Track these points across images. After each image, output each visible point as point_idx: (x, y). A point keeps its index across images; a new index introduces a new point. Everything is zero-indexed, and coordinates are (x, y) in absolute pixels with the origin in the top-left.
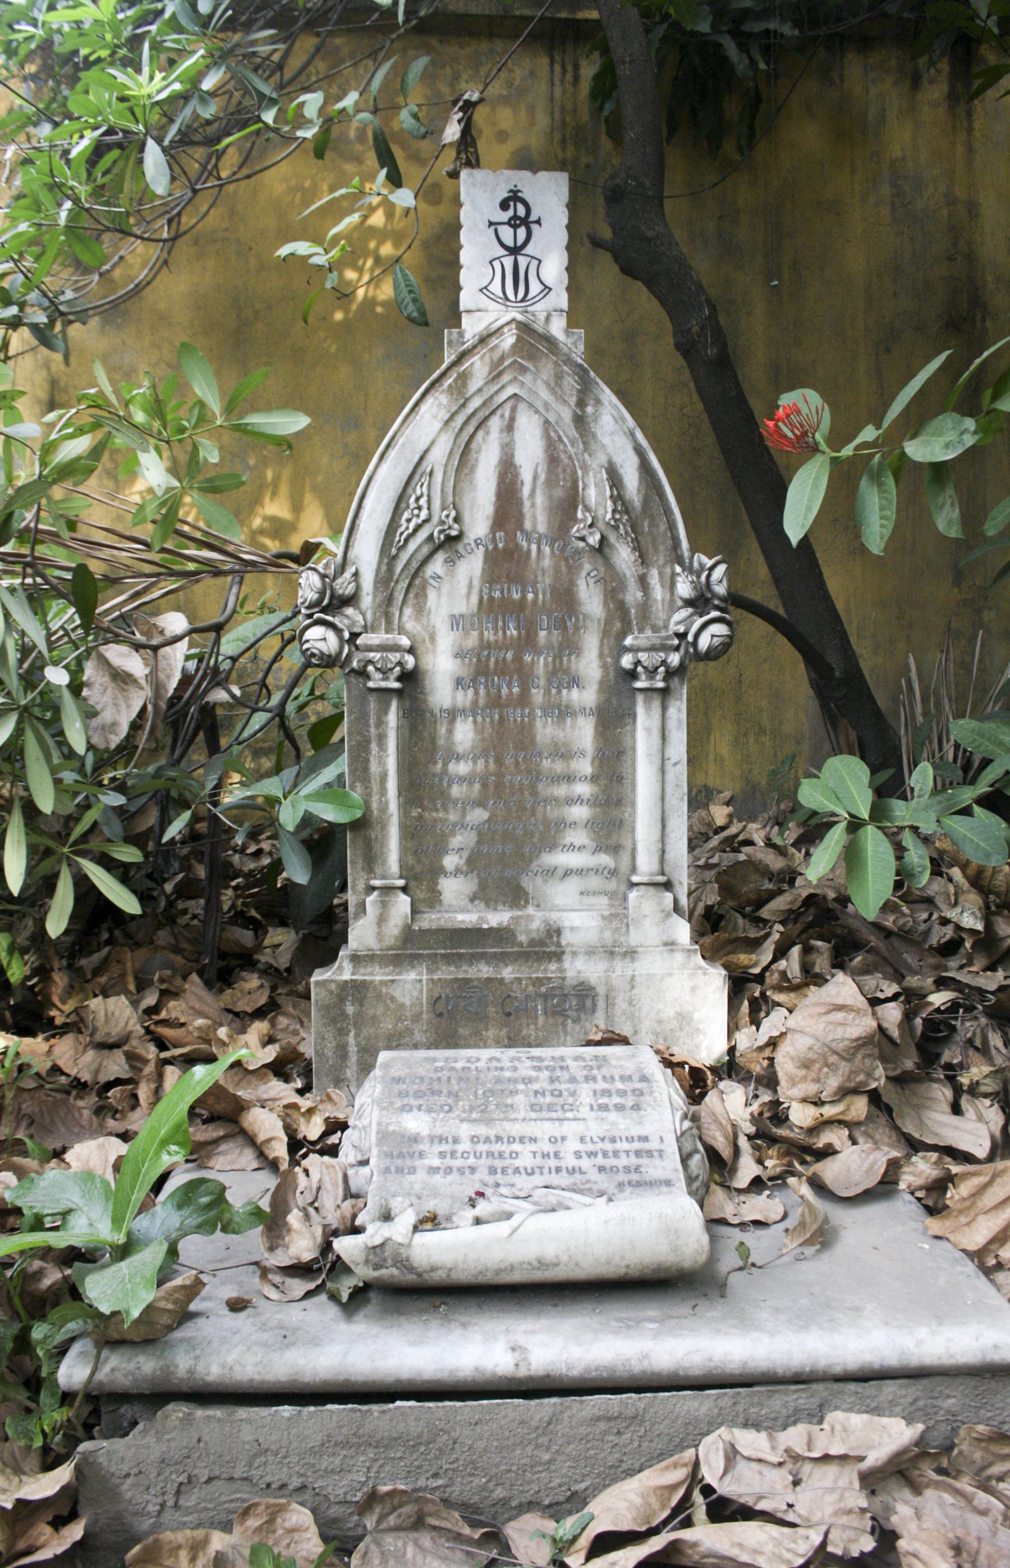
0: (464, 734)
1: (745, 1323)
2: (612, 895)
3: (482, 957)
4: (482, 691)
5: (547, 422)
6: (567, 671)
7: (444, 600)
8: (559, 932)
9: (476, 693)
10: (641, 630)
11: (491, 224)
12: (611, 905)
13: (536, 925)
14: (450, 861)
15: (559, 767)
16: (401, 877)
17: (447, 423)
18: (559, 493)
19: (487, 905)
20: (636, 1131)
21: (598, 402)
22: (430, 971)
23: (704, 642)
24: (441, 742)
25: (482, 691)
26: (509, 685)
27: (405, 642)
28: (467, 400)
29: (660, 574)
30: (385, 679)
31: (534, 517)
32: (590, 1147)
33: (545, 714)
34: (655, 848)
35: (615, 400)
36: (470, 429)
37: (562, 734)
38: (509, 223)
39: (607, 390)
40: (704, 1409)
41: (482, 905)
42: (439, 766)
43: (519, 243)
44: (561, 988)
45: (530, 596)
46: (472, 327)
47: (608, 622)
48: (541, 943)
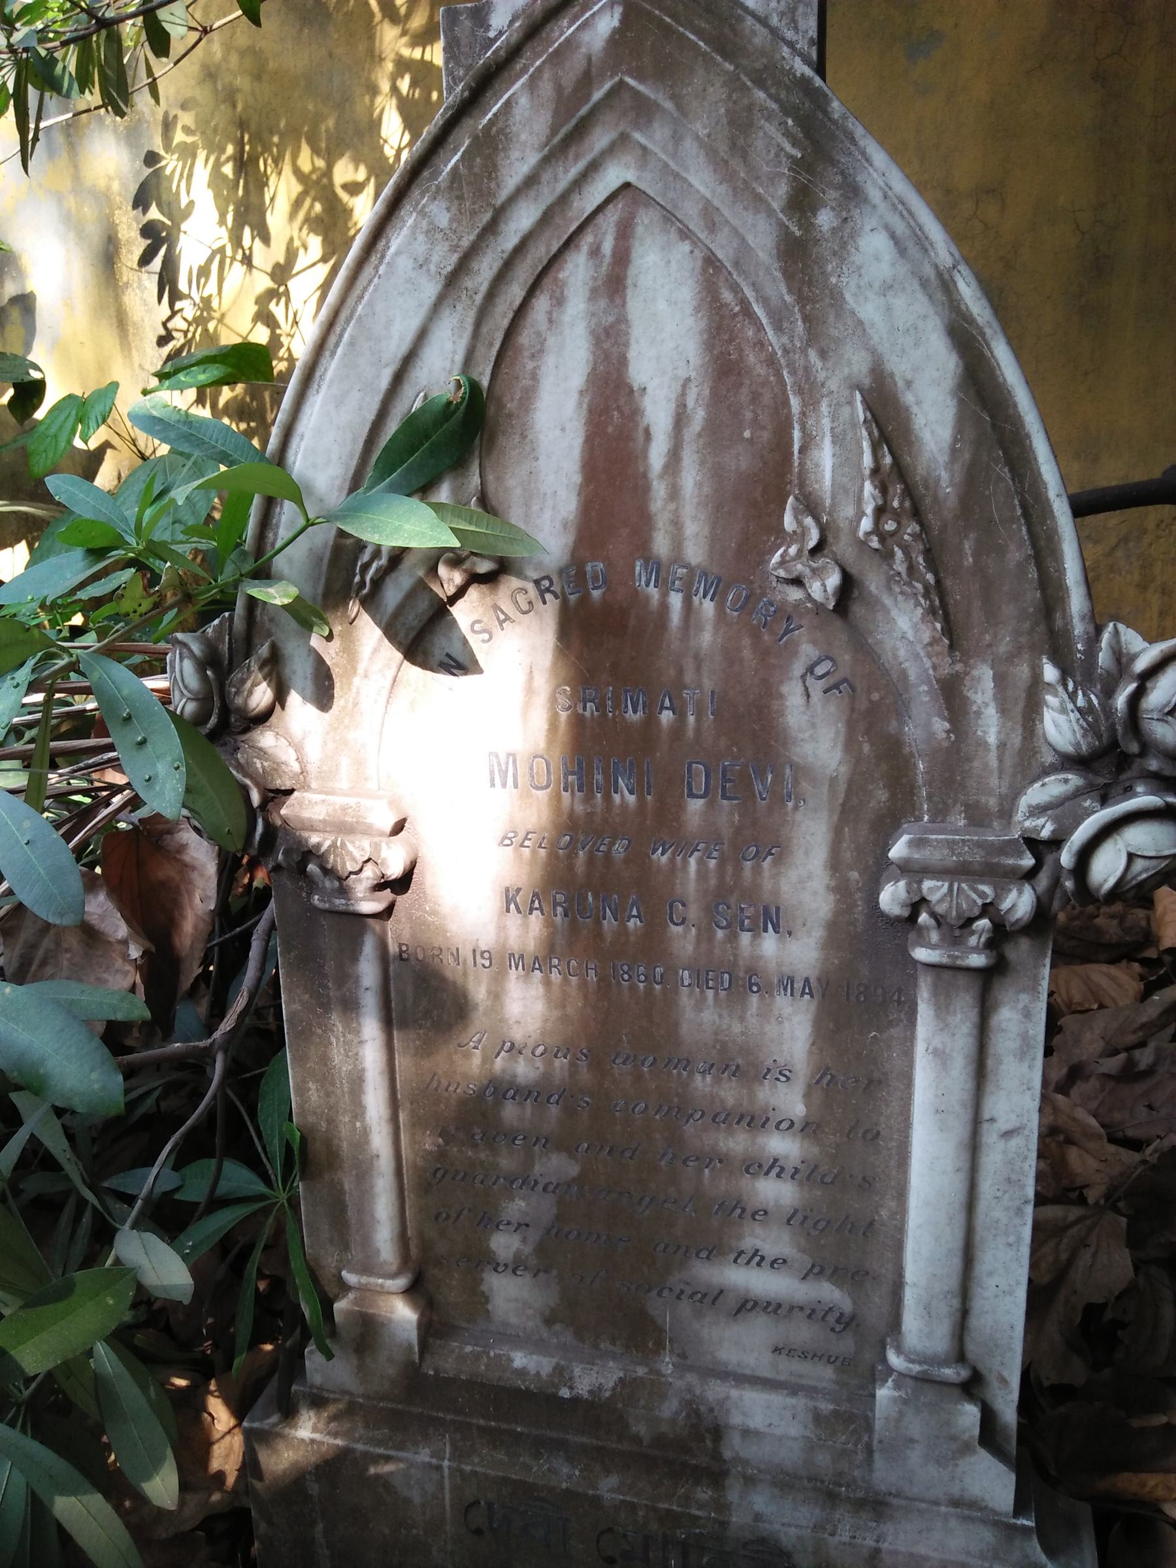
2: (844, 1365)
5: (711, 262)
6: (751, 894)
10: (940, 813)
13: (669, 1408)
15: (730, 1094)
17: (453, 280)
18: (740, 460)
19: (579, 1335)
21: (853, 193)
22: (459, 1454)
23: (1107, 867)
26: (620, 915)
28: (499, 215)
31: (677, 524)
33: (701, 979)
34: (946, 1309)
35: (901, 186)
36: (515, 292)
37: (737, 1028)
39: (879, 157)
41: (568, 1337)
45: (666, 717)
47: (856, 788)
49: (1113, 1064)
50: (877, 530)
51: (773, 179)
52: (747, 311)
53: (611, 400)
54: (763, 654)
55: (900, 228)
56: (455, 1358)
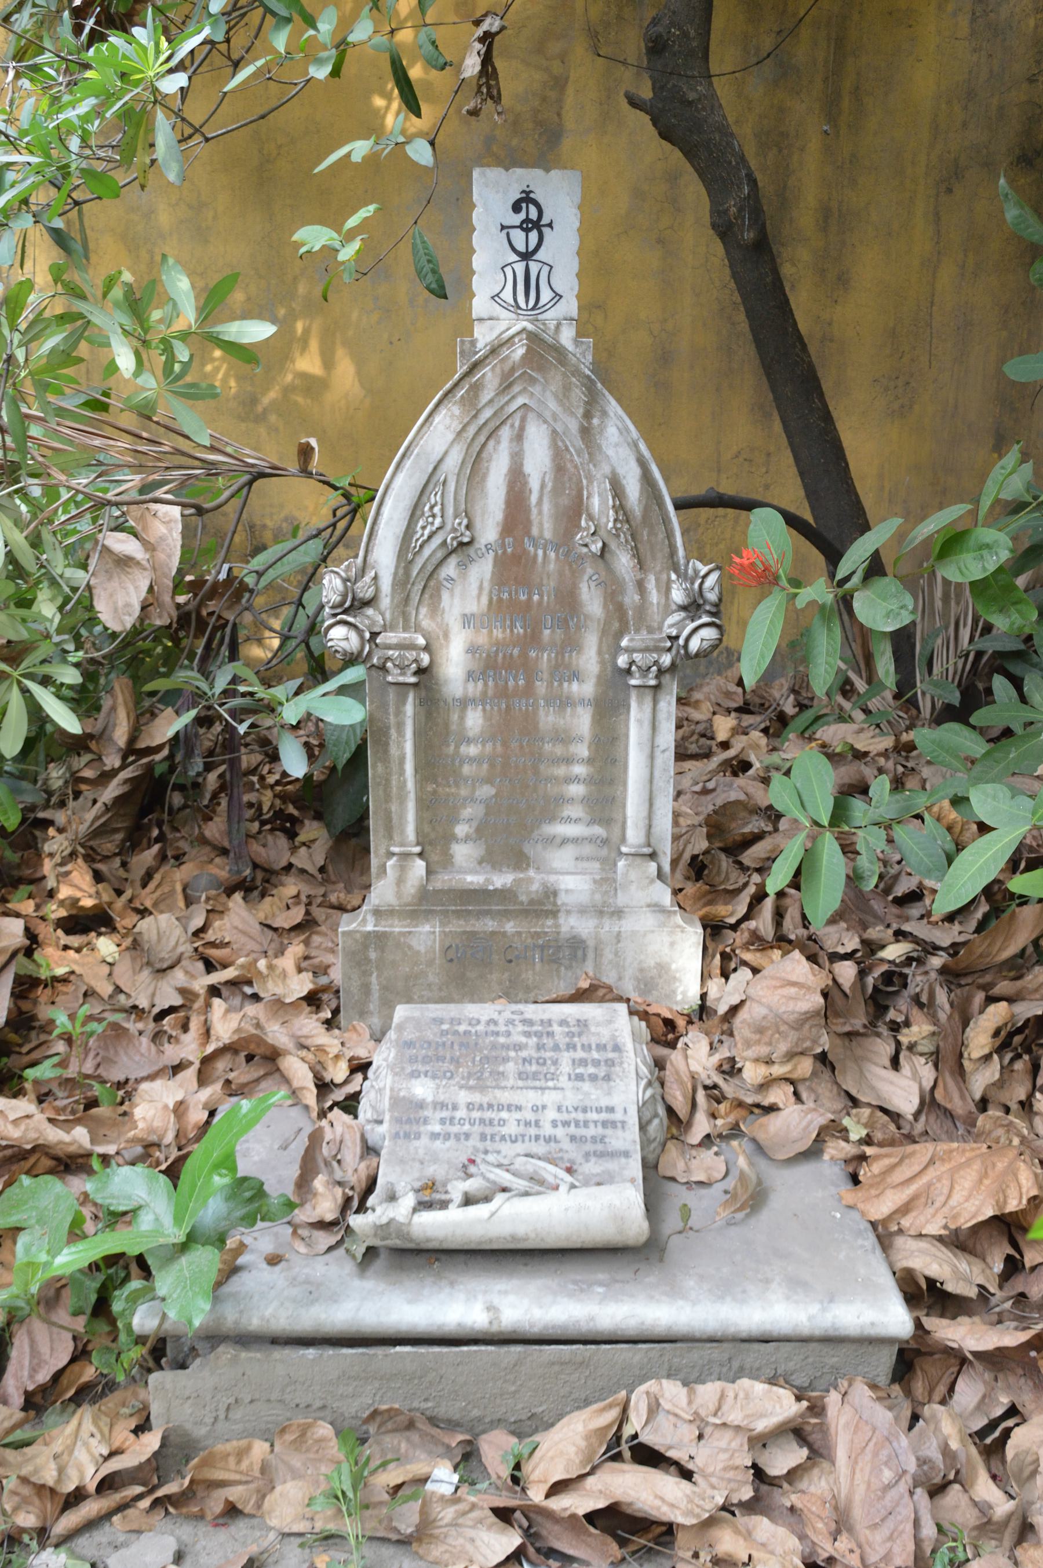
0: (474, 720)
1: (675, 1292)
2: (604, 861)
3: (488, 913)
4: (491, 683)
6: (568, 667)
7: (457, 601)
8: (555, 893)
9: (486, 684)
10: (637, 631)
11: (503, 227)
12: (603, 869)
13: (535, 887)
14: (461, 830)
15: (559, 750)
16: (418, 844)
17: (459, 434)
18: (565, 501)
19: (493, 867)
20: (604, 1102)
21: (604, 413)
23: (694, 645)
24: (454, 727)
25: (491, 683)
27: (421, 641)
28: (478, 412)
29: (657, 580)
30: (403, 674)
31: (541, 524)
32: (565, 1117)
33: (548, 704)
34: (642, 824)
35: (620, 411)
36: (482, 439)
37: (562, 722)
38: (520, 227)
39: (613, 402)
40: (637, 1358)
41: (489, 868)
42: (452, 748)
43: (531, 249)
44: (556, 941)
45: (536, 598)
46: (483, 336)
47: (607, 622)
48: (540, 903)
49: (698, 788)
50: (615, 527)
51: (578, 407)
52: (567, 449)
53: (517, 479)
54: (573, 572)
55: (620, 425)
56: (443, 880)
